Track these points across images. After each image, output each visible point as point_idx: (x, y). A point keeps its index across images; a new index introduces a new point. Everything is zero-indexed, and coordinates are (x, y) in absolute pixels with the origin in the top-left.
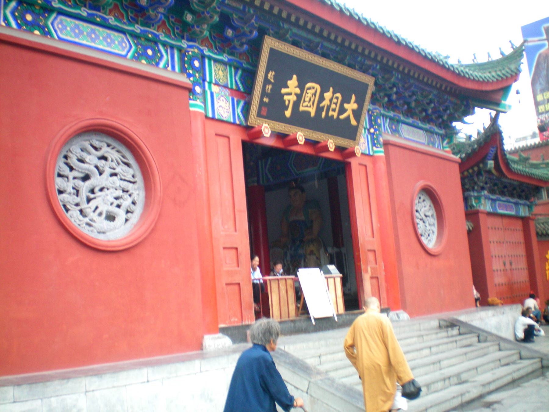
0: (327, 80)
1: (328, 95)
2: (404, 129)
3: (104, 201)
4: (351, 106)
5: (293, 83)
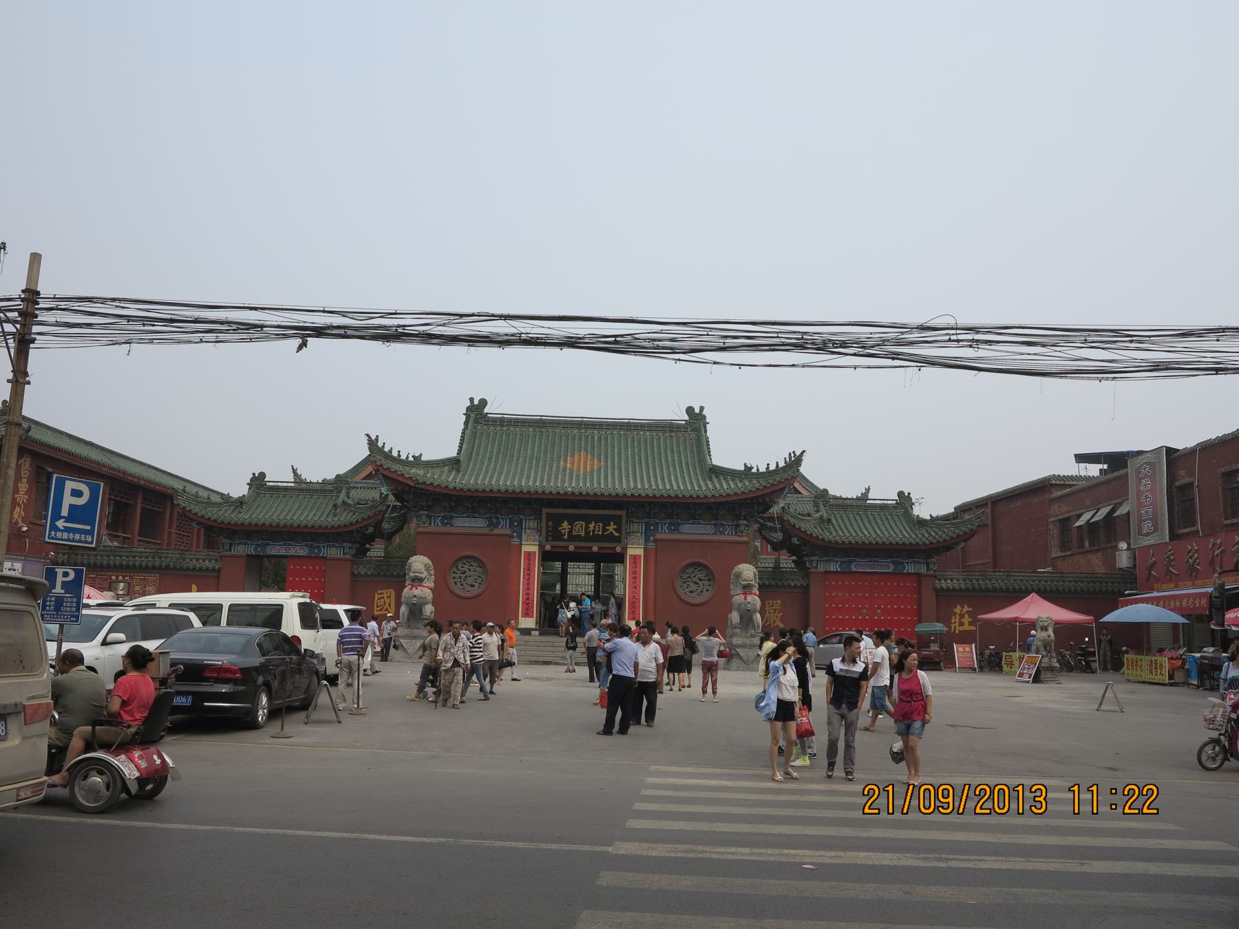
0: (587, 519)
1: (592, 526)
2: (686, 528)
3: (470, 580)
4: (612, 528)
5: (565, 524)
